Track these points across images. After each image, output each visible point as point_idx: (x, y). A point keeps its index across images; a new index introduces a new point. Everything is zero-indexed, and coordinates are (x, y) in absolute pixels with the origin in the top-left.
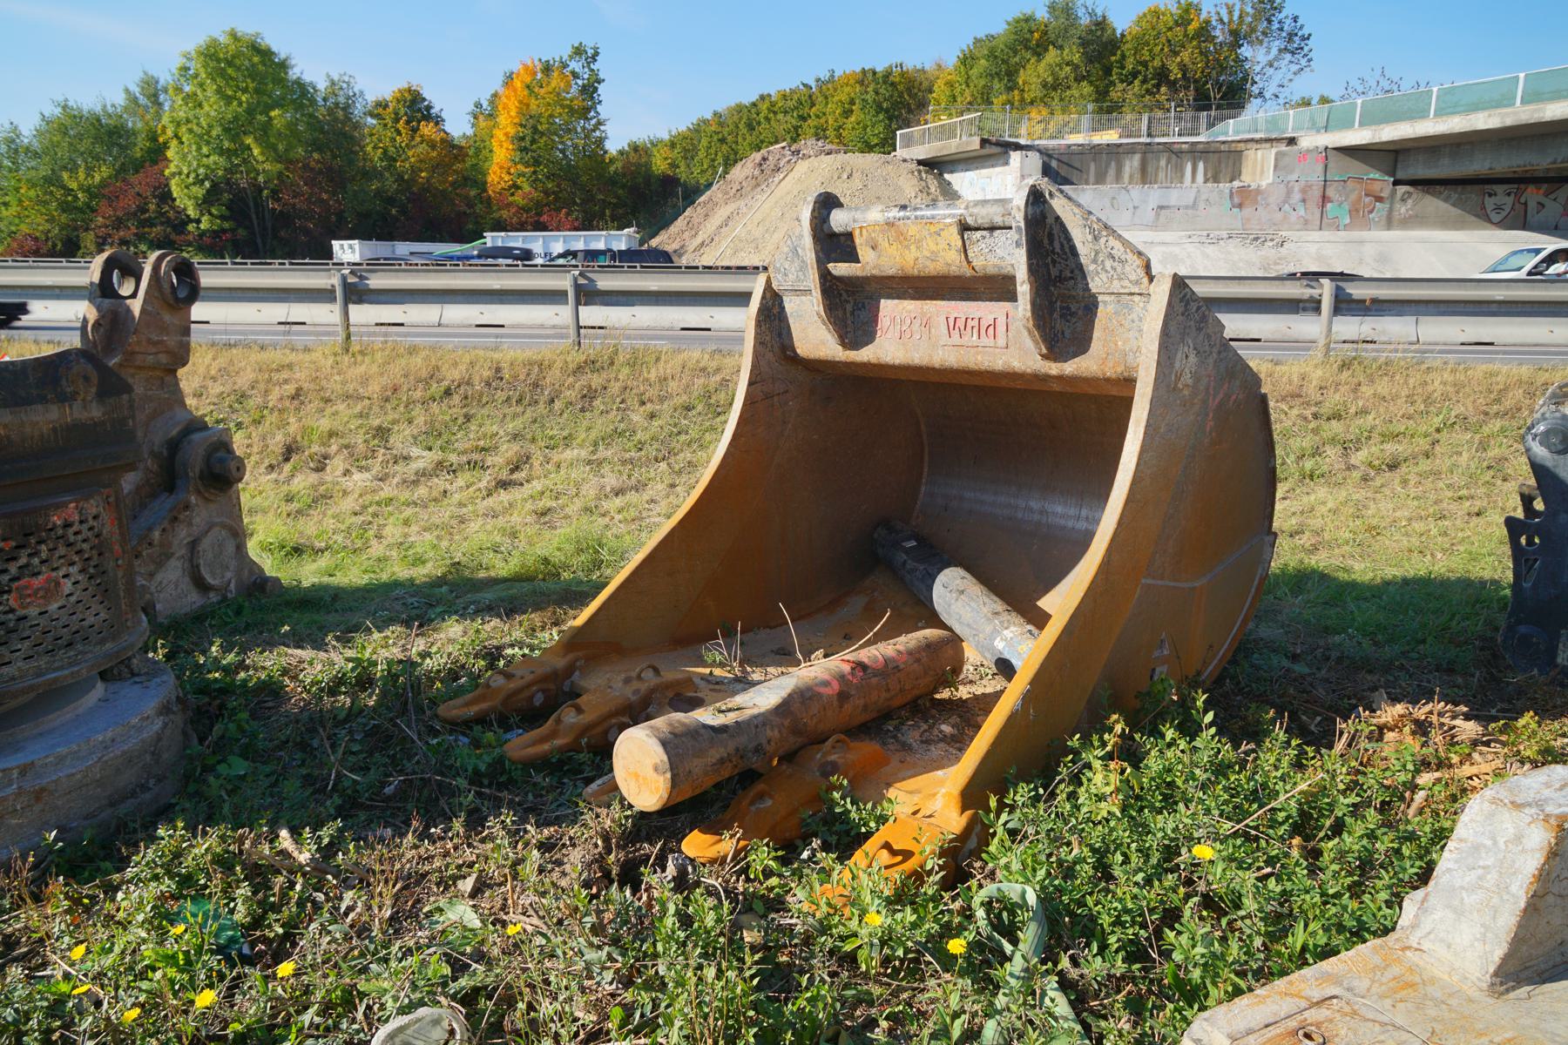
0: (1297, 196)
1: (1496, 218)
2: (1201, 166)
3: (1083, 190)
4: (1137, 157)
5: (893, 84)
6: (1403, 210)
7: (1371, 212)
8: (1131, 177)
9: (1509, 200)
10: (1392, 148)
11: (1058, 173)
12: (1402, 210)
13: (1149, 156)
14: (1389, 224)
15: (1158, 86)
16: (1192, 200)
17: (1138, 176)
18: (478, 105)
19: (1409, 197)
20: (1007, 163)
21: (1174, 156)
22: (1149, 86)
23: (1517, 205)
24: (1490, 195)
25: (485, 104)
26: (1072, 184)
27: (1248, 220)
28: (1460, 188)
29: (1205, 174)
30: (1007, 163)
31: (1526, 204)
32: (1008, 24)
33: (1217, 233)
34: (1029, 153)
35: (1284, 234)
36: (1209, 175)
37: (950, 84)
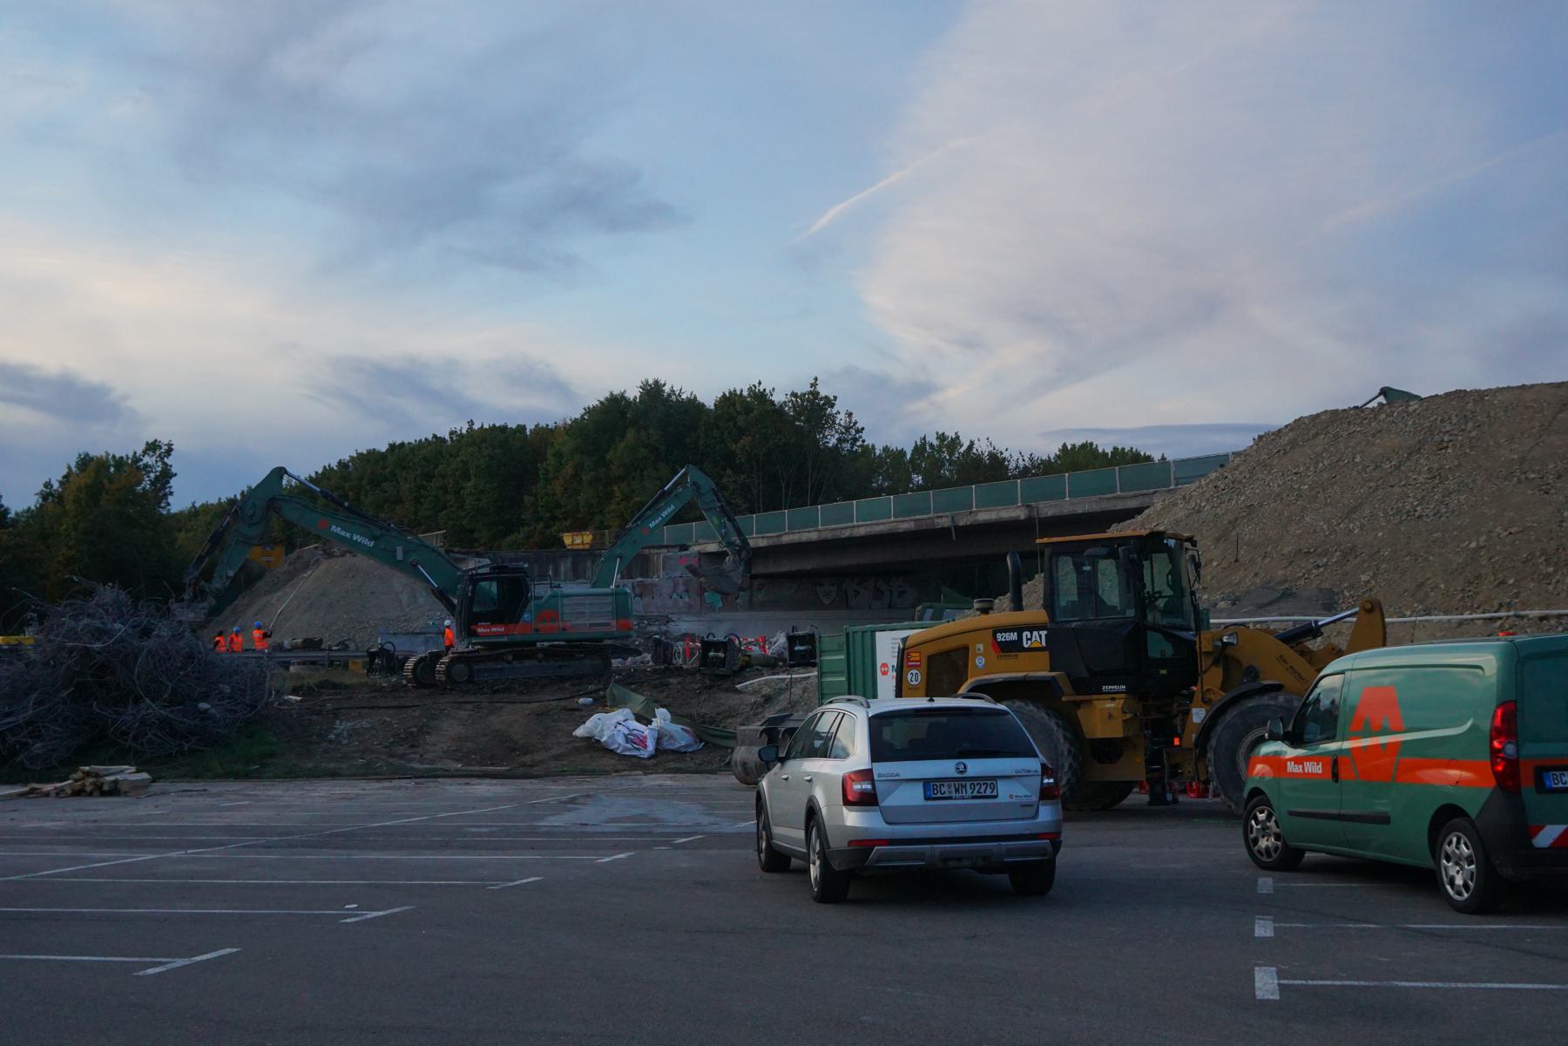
0: (681, 588)
1: (826, 601)
4: (569, 560)
6: (760, 597)
7: (737, 598)
12: (760, 597)
14: (751, 606)
18: (48, 485)
24: (820, 586)
25: (56, 485)
32: (585, 409)
37: (558, 455)
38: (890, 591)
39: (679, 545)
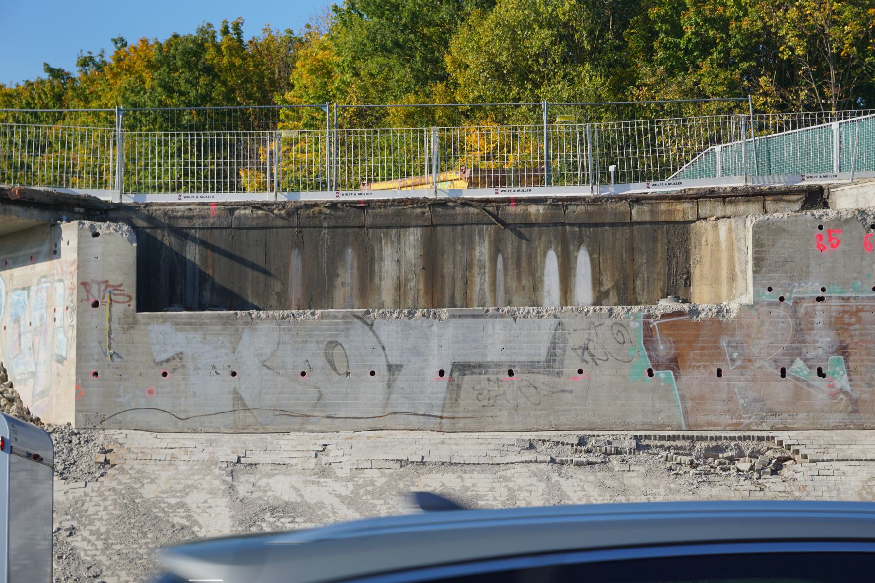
2: (583, 260)
3: (250, 323)
4: (413, 238)
5: (209, 70)
8: (400, 286)
11: (203, 277)
13: (445, 234)
15: (752, 75)
16: (544, 351)
17: (417, 285)
20: (54, 253)
21: (509, 236)
22: (736, 75)
26: (243, 305)
27: (701, 400)
29: (597, 282)
30: (54, 253)
33: (607, 435)
34: (102, 227)
35: (786, 437)
36: (607, 284)
37: (323, 71)
39: (800, 191)
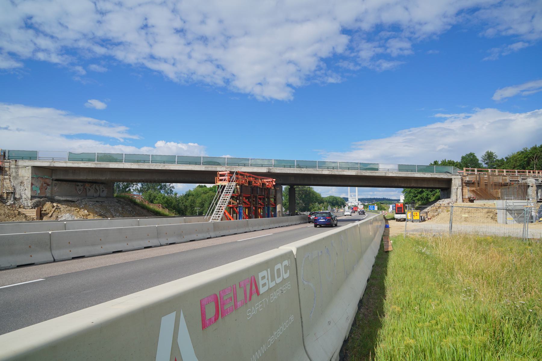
6: (55, 189)
7: (46, 189)
9: (82, 188)
10: (51, 168)
19: (57, 185)
23: (84, 189)
24: (78, 186)
28: (70, 183)
31: (86, 189)
38: (100, 190)
